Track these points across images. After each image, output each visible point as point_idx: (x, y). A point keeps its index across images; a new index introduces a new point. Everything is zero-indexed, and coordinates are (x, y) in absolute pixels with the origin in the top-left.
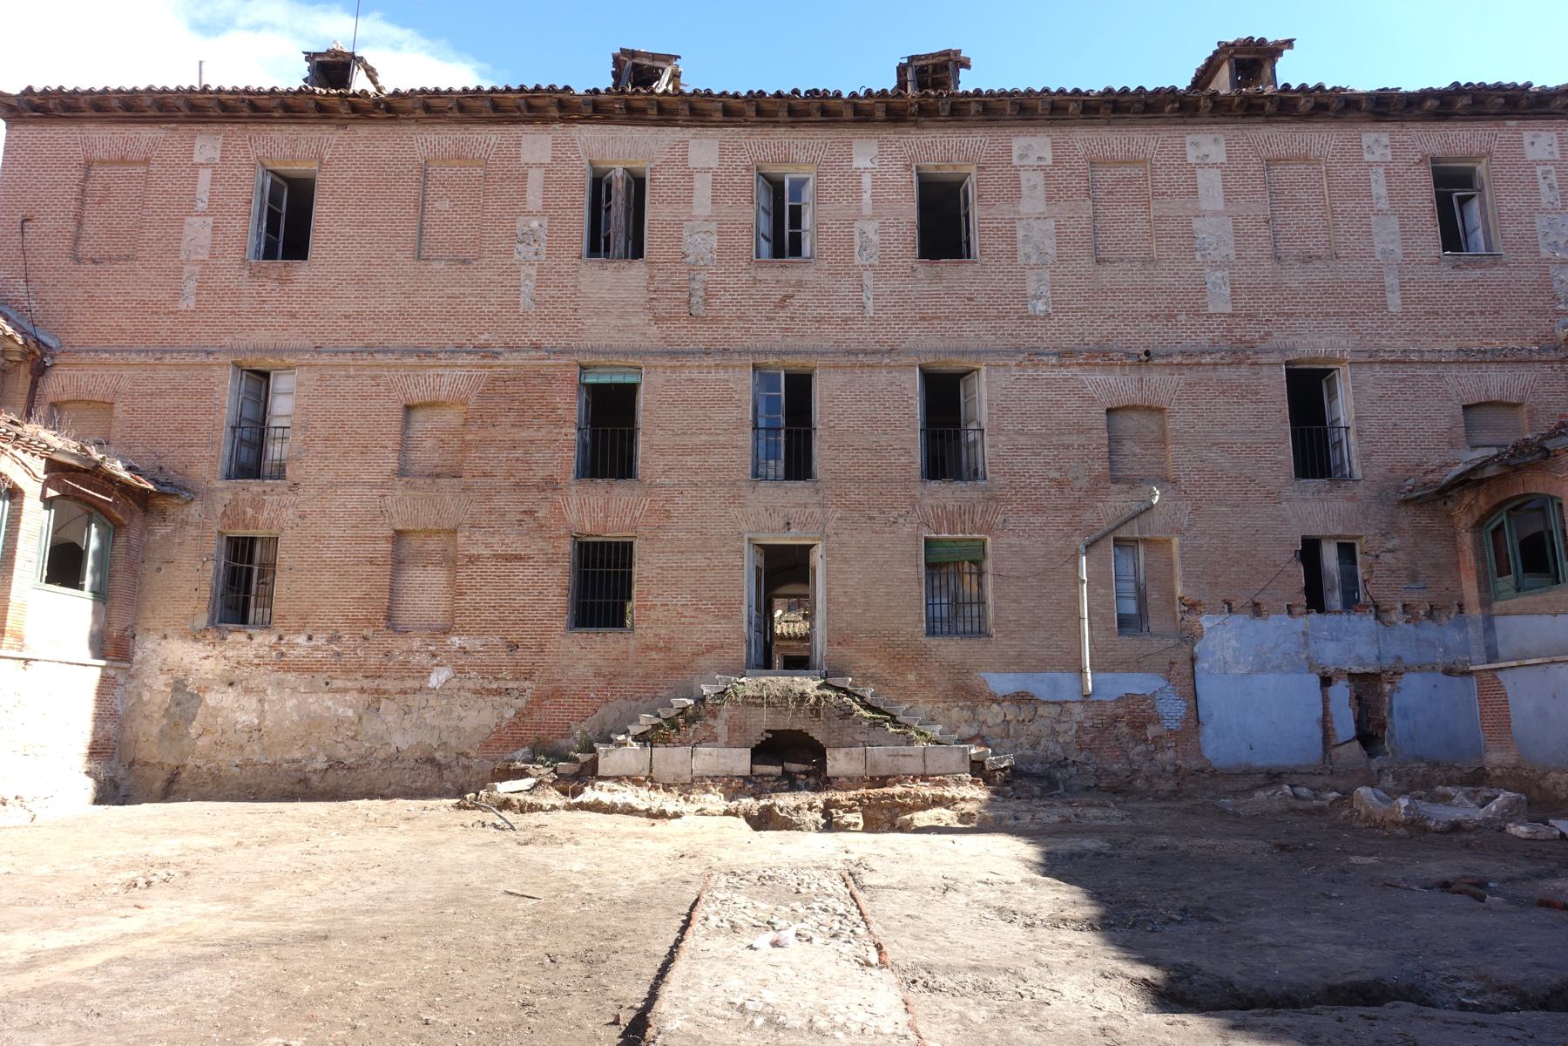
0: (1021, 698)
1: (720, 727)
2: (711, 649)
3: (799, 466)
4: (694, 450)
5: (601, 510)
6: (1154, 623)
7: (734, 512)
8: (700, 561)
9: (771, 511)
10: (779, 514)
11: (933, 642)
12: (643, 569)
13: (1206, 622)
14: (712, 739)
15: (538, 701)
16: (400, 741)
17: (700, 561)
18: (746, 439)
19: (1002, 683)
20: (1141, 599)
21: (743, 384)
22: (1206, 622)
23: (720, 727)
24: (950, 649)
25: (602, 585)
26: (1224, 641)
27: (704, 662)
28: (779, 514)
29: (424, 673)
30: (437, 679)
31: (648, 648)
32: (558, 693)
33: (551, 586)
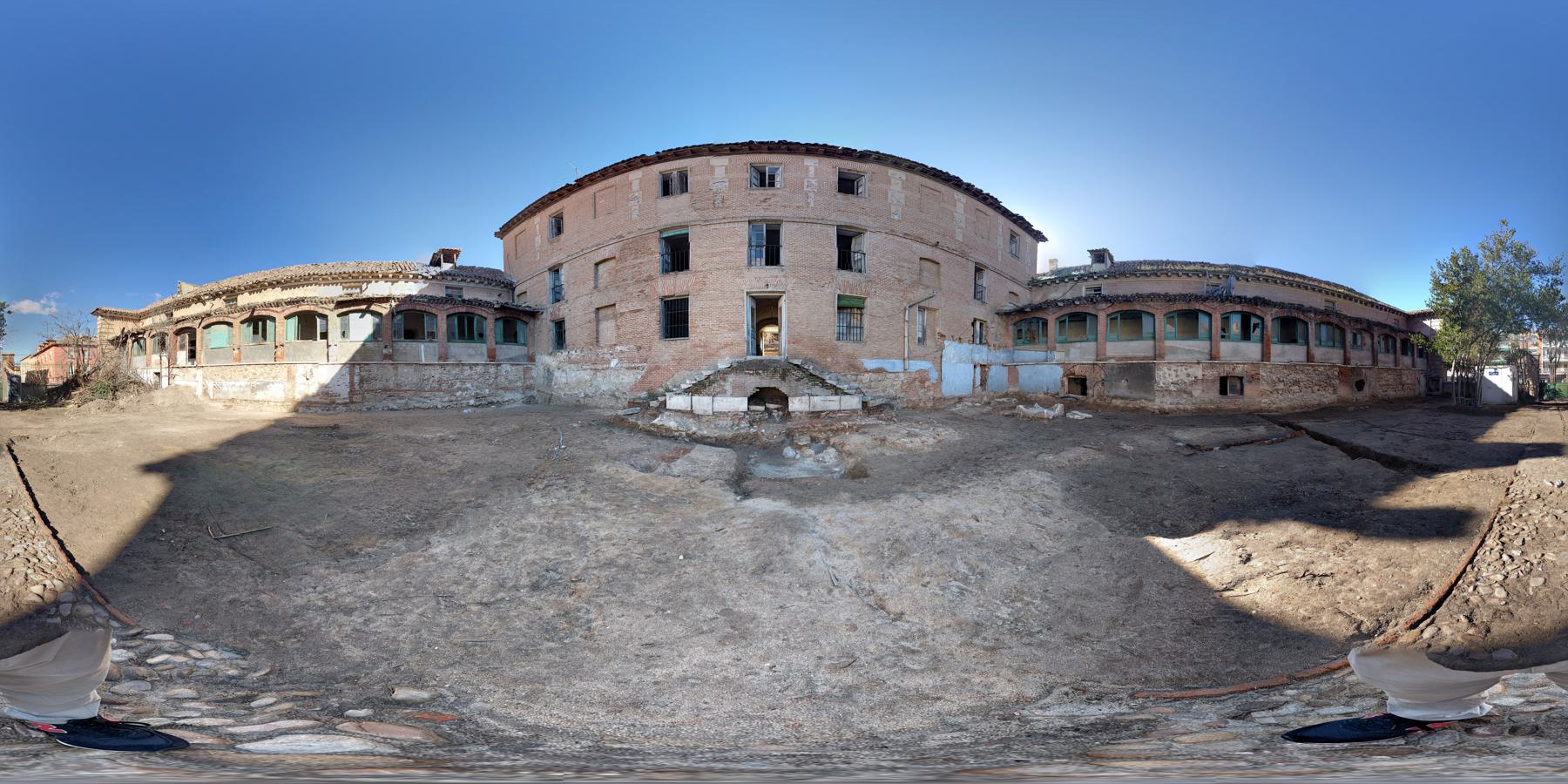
0: (879, 371)
1: (728, 387)
2: (726, 345)
3: (773, 258)
4: (719, 254)
5: (675, 285)
6: (928, 342)
7: (738, 280)
8: (721, 303)
9: (758, 279)
10: (763, 279)
11: (840, 343)
12: (694, 309)
13: (946, 343)
14: (724, 392)
15: (650, 371)
16: (604, 388)
17: (721, 303)
18: (745, 249)
19: (870, 364)
20: (924, 332)
21: (744, 229)
22: (946, 343)
23: (728, 387)
24: (847, 347)
25: (676, 319)
26: (951, 350)
27: (723, 352)
28: (763, 279)
29: (609, 362)
30: (614, 363)
31: (696, 346)
32: (657, 368)
33: (652, 320)
